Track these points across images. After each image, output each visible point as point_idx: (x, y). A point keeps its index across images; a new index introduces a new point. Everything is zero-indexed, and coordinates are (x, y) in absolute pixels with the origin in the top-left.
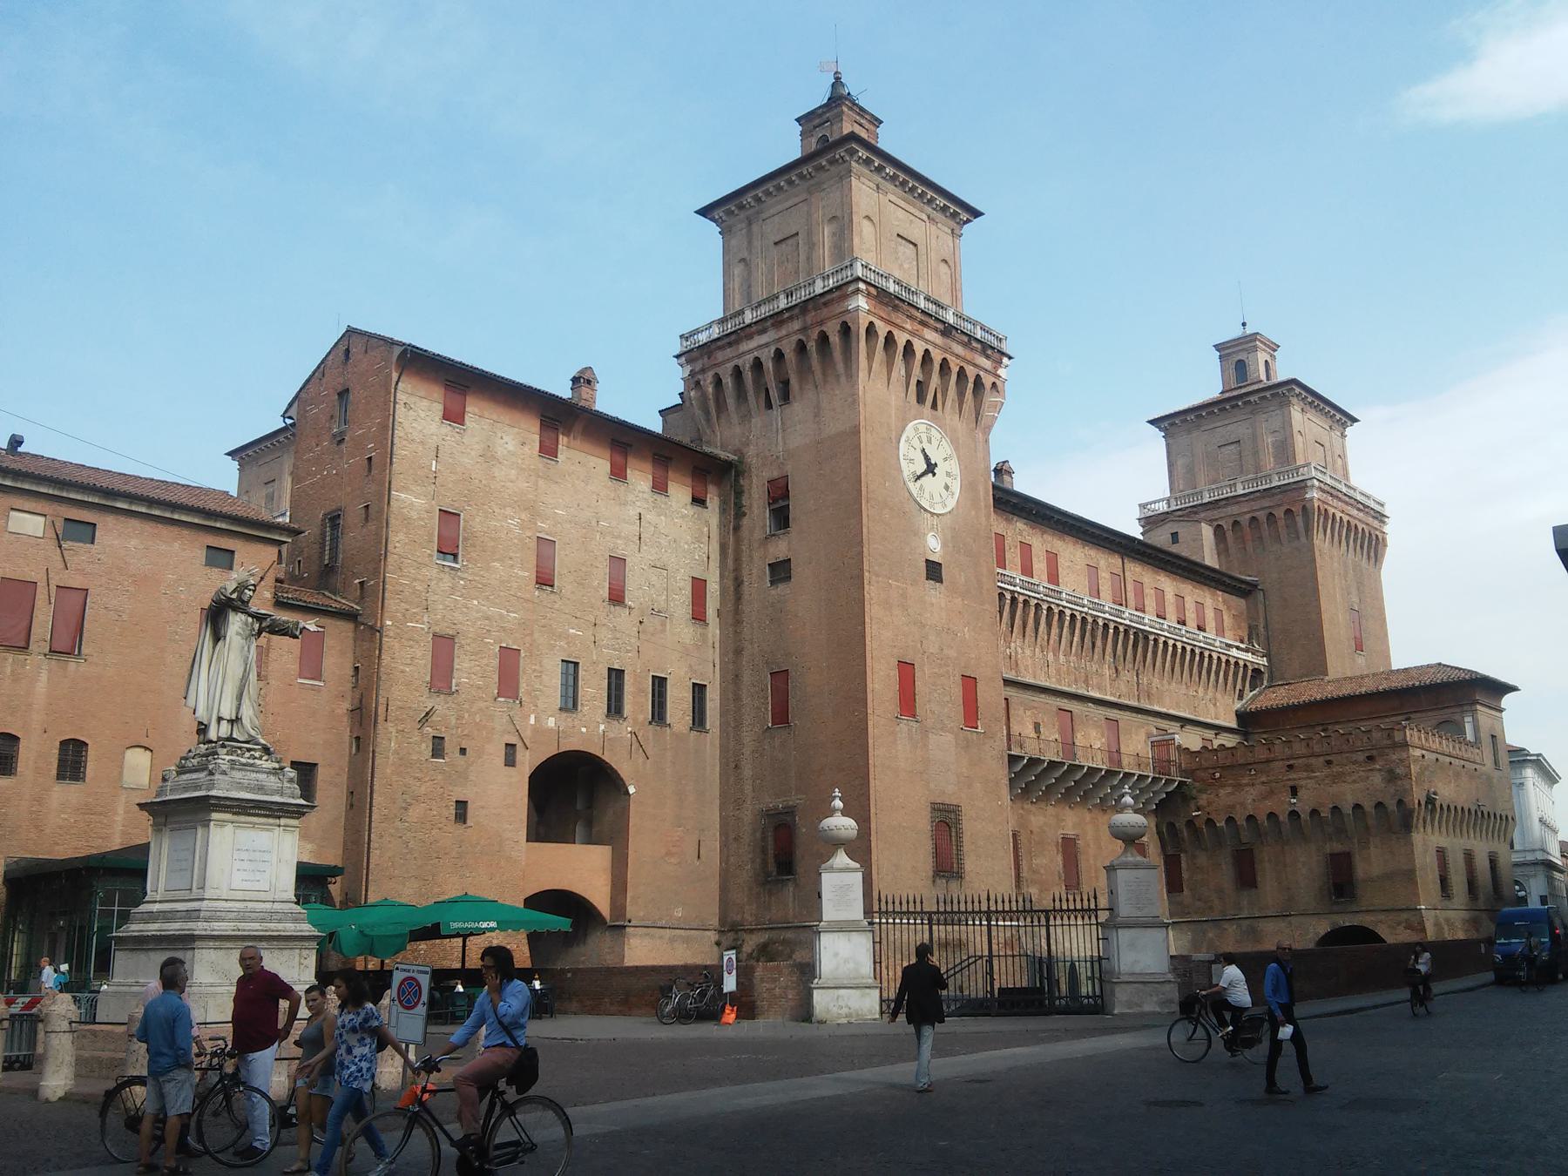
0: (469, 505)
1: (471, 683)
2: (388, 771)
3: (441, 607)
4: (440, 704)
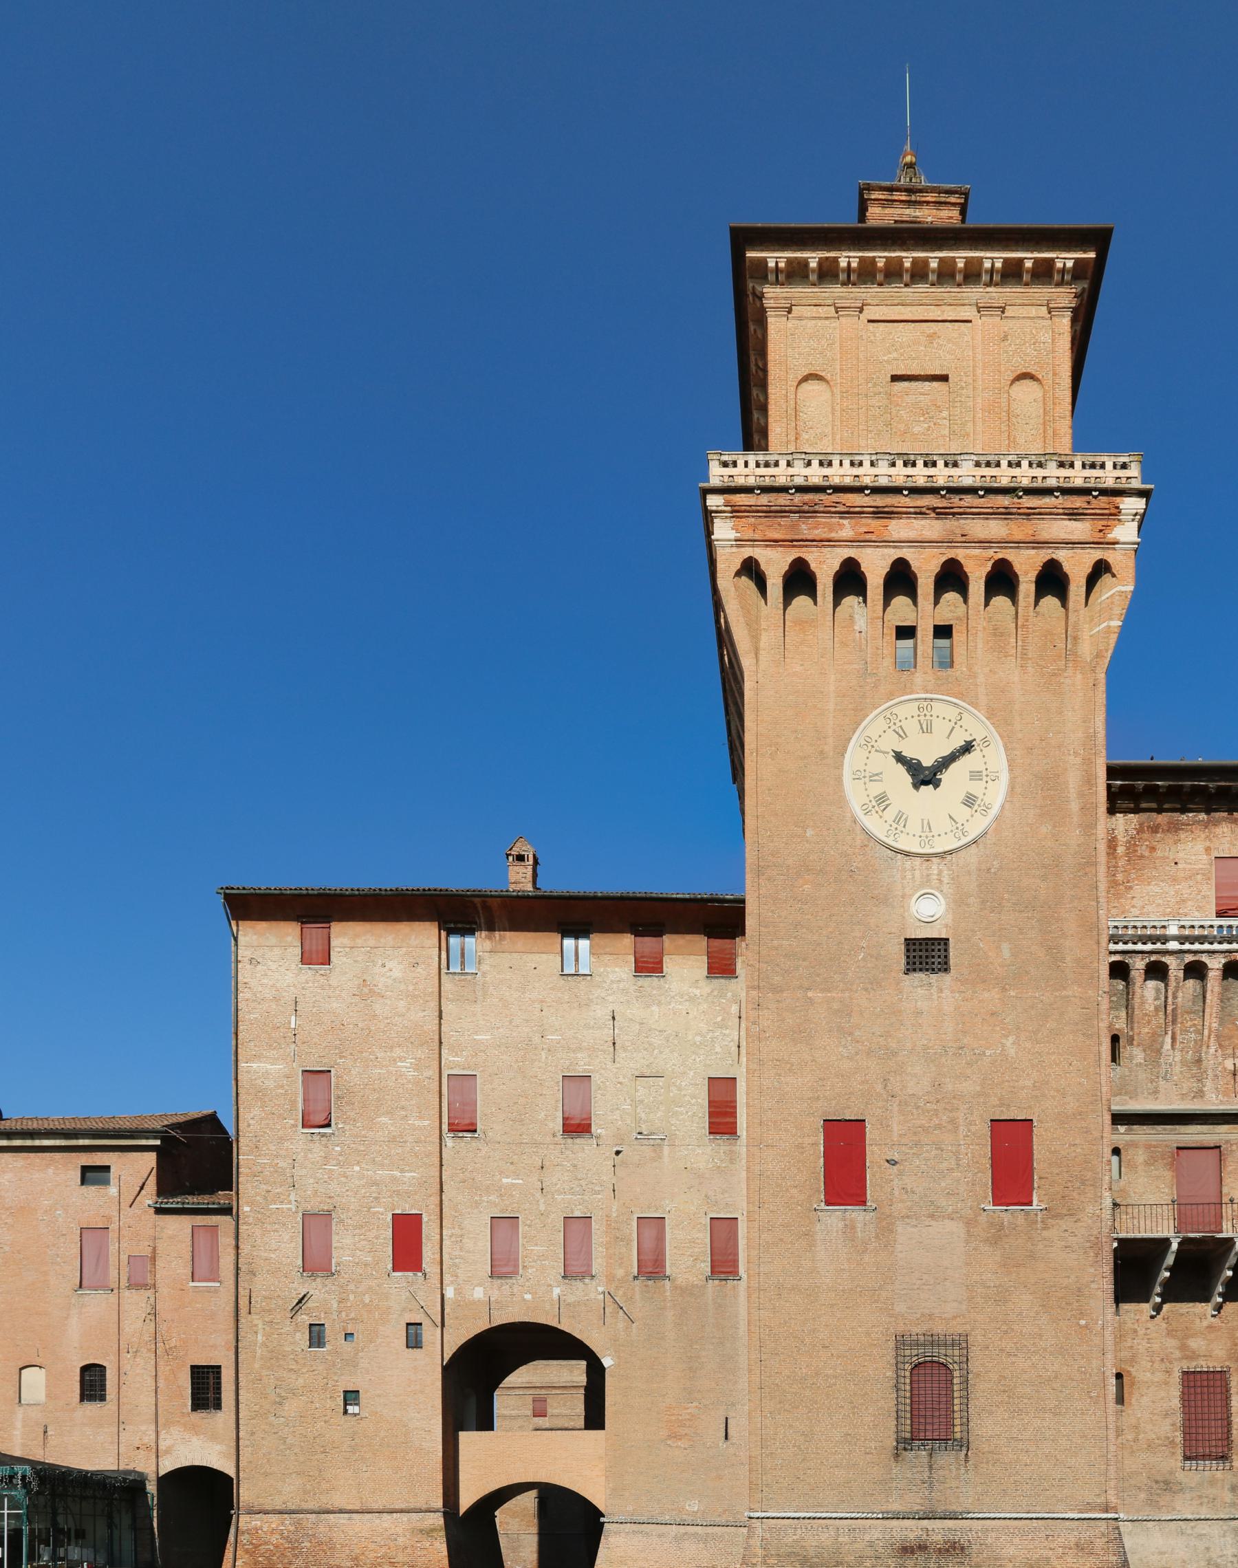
0: (341, 1057)
1: (357, 1260)
2: (257, 1366)
3: (311, 1181)
4: (317, 1289)
